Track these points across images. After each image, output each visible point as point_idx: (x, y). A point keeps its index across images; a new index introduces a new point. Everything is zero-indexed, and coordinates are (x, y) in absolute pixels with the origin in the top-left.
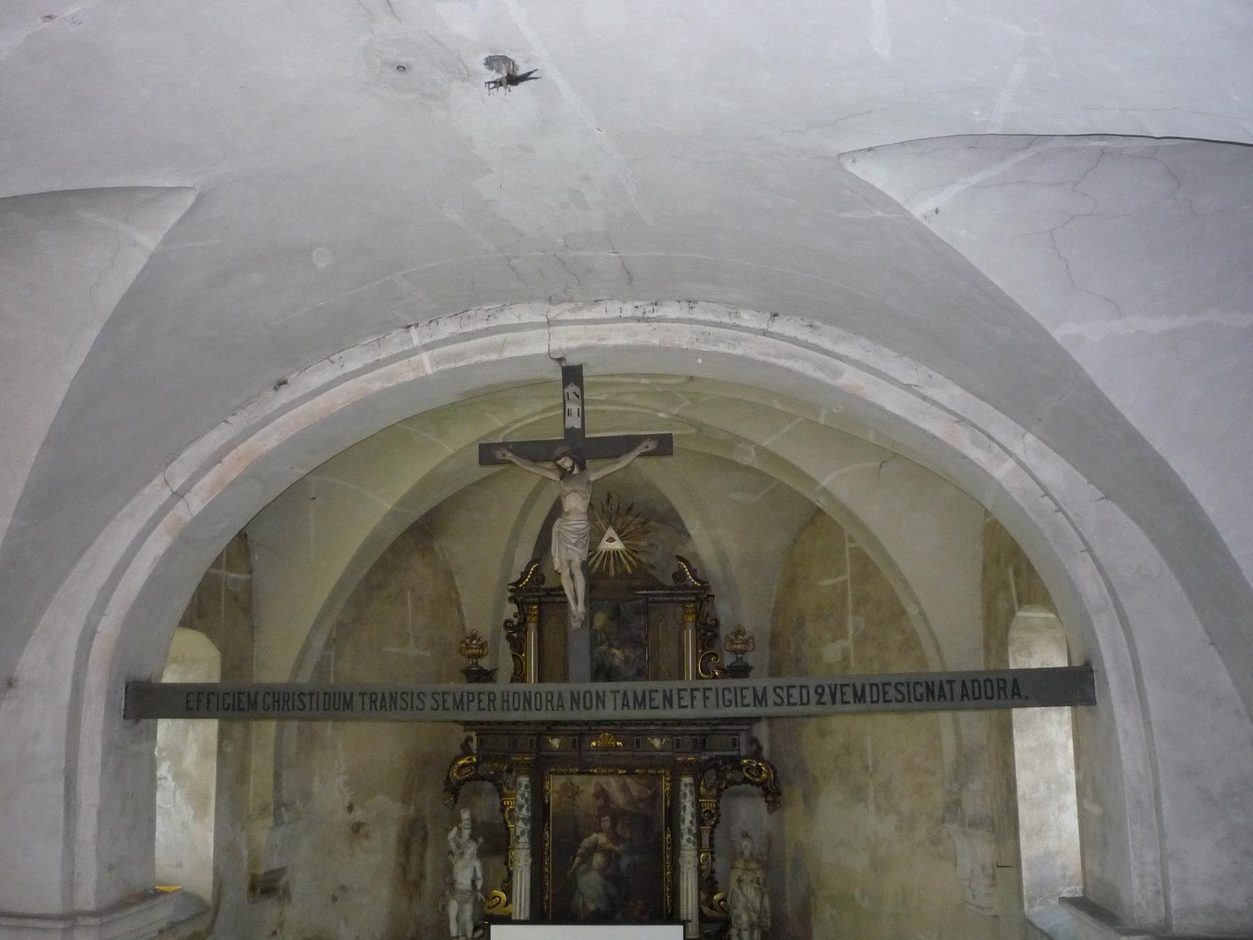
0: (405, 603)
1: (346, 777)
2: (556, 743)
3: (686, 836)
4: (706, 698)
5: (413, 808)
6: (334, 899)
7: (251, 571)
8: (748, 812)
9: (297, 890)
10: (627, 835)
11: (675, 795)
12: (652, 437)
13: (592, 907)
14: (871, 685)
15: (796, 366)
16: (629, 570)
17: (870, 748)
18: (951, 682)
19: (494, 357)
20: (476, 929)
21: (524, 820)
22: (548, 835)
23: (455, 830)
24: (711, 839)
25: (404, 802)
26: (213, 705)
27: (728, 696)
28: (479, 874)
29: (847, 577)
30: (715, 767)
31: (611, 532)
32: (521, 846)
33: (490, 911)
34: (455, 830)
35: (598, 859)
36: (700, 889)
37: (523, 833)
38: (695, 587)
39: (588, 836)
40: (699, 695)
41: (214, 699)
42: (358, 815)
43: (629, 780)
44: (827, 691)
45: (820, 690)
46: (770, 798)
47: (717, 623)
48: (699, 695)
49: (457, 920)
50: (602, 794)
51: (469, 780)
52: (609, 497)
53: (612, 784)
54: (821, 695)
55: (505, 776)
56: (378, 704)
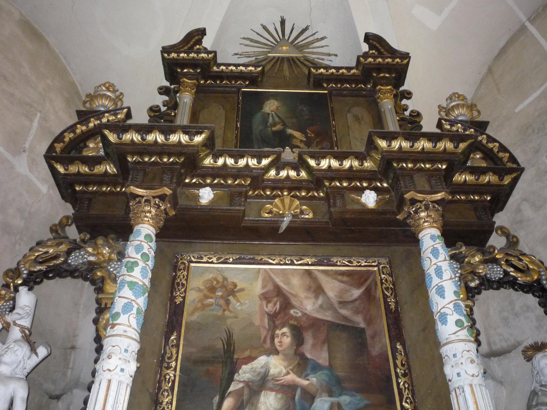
0: (32, 121)
10: (322, 357)
21: (132, 285)
37: (127, 308)
39: (251, 359)
52: (283, 22)
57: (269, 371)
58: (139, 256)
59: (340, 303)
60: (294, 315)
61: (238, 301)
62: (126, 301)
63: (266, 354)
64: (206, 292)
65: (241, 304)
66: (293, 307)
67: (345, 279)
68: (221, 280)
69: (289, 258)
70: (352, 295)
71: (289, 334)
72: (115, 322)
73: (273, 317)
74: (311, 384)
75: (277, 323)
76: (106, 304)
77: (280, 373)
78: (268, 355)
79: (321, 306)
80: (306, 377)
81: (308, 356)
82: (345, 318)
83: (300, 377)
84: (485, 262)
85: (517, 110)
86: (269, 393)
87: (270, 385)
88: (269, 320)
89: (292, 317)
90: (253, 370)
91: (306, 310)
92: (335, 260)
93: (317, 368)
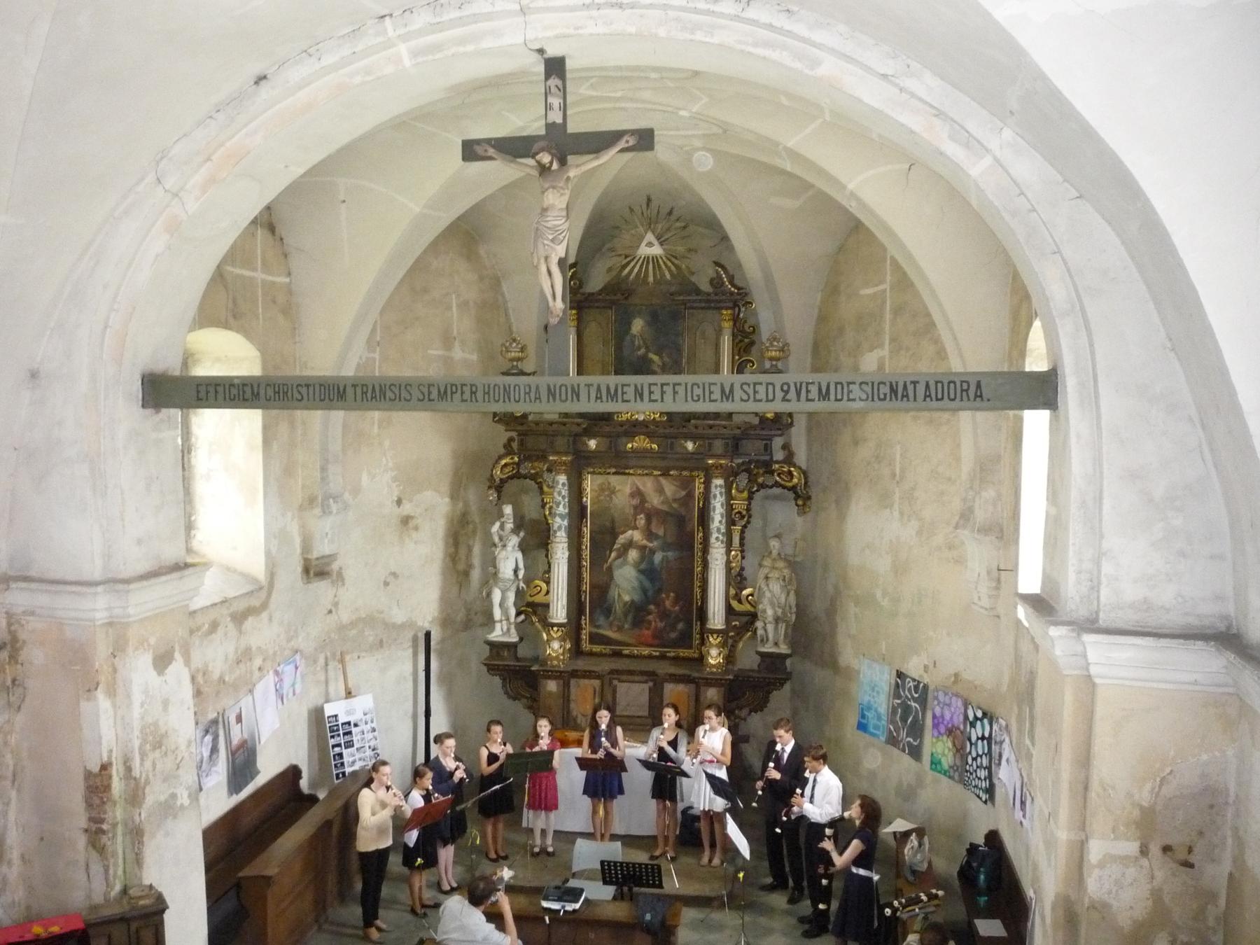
1: (394, 474)
2: (592, 444)
3: (715, 535)
4: (675, 393)
5: (461, 505)
6: (386, 584)
7: (289, 274)
8: (779, 513)
9: (349, 574)
10: (661, 533)
11: (707, 496)
12: (632, 132)
13: (627, 598)
14: (837, 384)
15: (774, 55)
16: (668, 277)
17: (898, 456)
18: (915, 383)
19: (470, 48)
20: (518, 614)
22: (587, 531)
23: (497, 525)
24: (742, 539)
25: (452, 497)
26: (220, 396)
27: (698, 391)
28: (521, 565)
29: (886, 286)
30: (748, 471)
31: (650, 237)
32: (558, 540)
33: (530, 599)
34: (497, 525)
35: (633, 554)
36: (728, 584)
37: (560, 528)
38: (732, 294)
40: (668, 389)
41: (220, 389)
42: (407, 508)
43: (663, 480)
44: (793, 388)
45: (785, 388)
46: (800, 502)
47: (755, 329)
48: (668, 389)
49: (501, 605)
50: (637, 493)
51: (511, 478)
53: (647, 485)
54: (787, 392)
55: (546, 475)
56: (369, 395)
73: (635, 508)
84: (766, 472)
85: (863, 292)
93: (657, 537)
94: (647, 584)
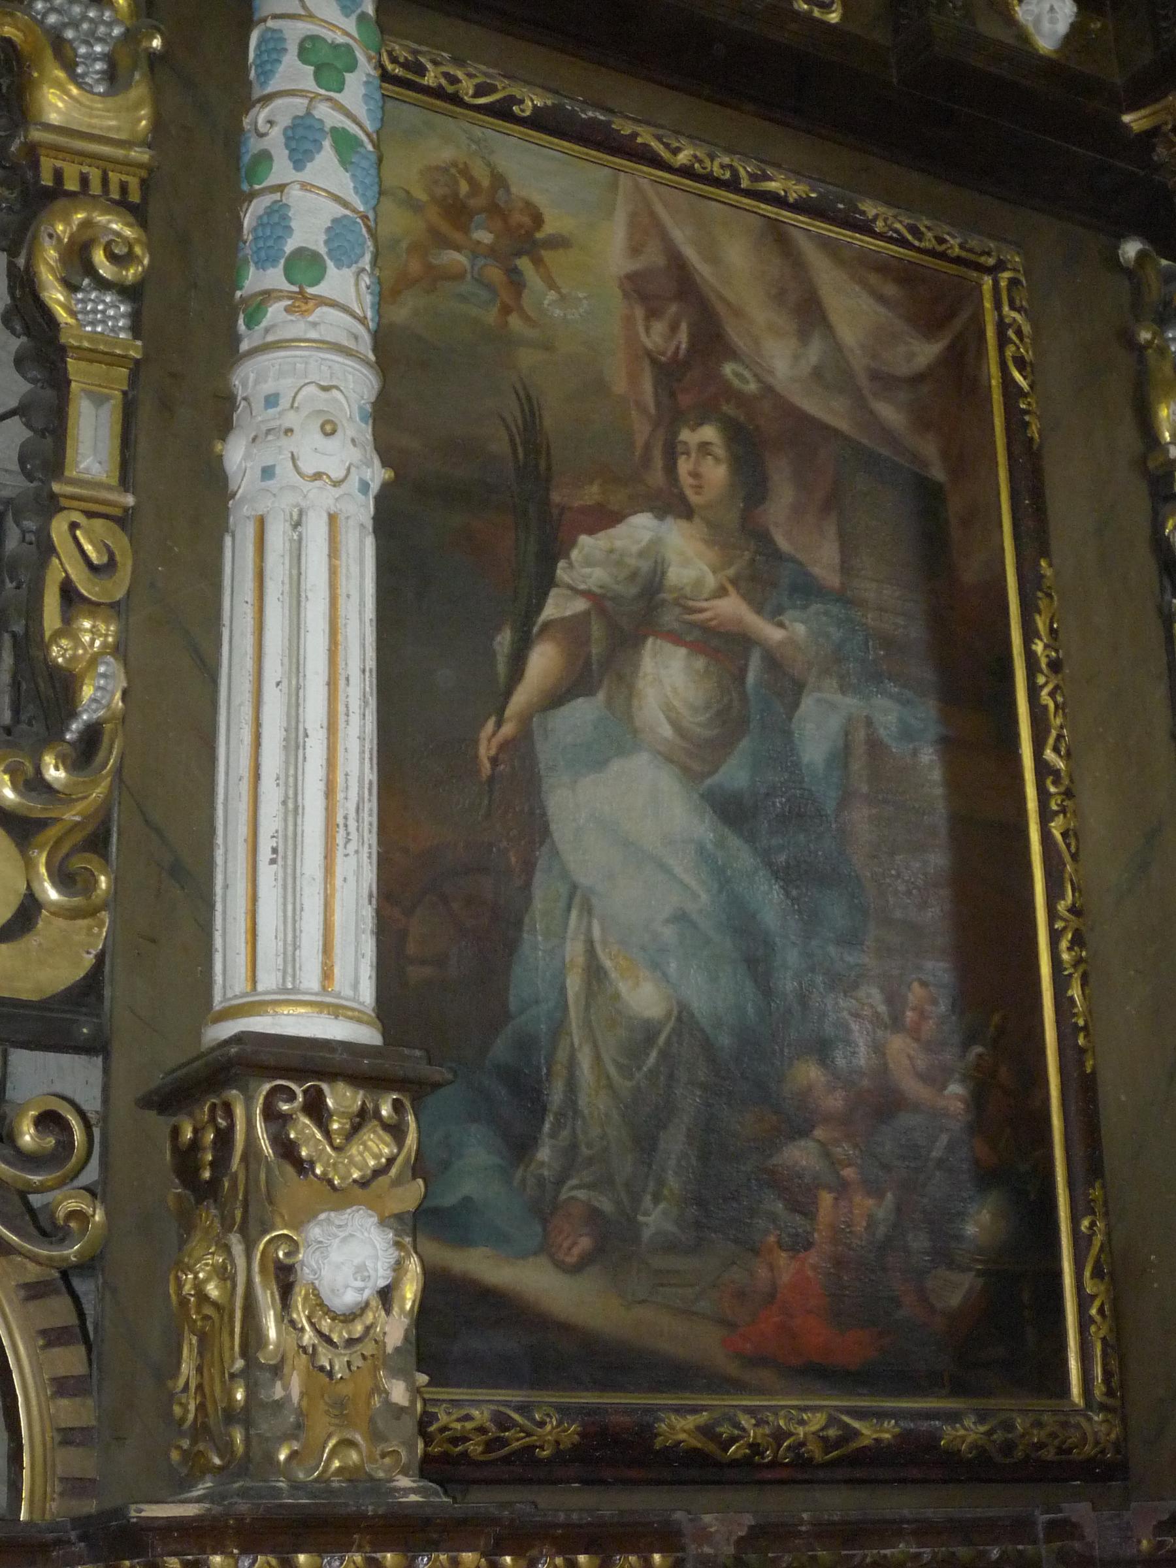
10: (823, 560)
13: (644, 998)
35: (668, 680)
39: (604, 518)
57: (663, 573)
58: (350, 24)
59: (875, 376)
60: (736, 382)
61: (552, 285)
62: (341, 211)
63: (651, 510)
64: (433, 214)
65: (563, 297)
66: (732, 354)
67: (891, 290)
68: (486, 183)
69: (726, 160)
70: (910, 357)
71: (720, 451)
72: (311, 291)
73: (669, 373)
74: (791, 641)
75: (685, 400)
76: (58, 175)
77: (699, 583)
78: (661, 512)
79: (817, 373)
80: (775, 615)
81: (782, 543)
82: (887, 434)
83: (759, 610)
86: (668, 647)
87: (669, 618)
88: (657, 384)
89: (729, 393)
90: (614, 557)
91: (771, 372)
92: (870, 208)
93: (806, 590)
94: (769, 901)
